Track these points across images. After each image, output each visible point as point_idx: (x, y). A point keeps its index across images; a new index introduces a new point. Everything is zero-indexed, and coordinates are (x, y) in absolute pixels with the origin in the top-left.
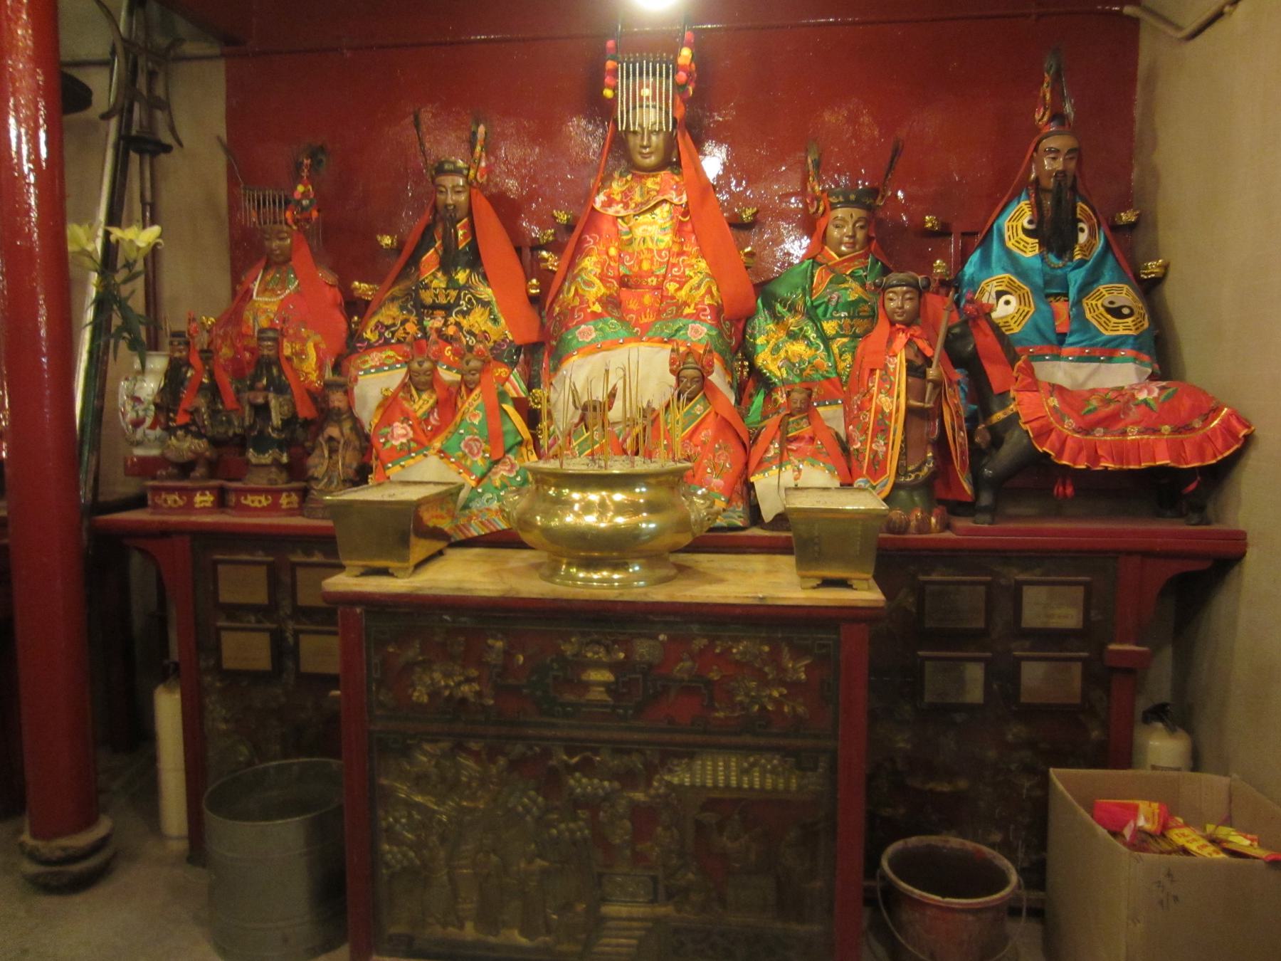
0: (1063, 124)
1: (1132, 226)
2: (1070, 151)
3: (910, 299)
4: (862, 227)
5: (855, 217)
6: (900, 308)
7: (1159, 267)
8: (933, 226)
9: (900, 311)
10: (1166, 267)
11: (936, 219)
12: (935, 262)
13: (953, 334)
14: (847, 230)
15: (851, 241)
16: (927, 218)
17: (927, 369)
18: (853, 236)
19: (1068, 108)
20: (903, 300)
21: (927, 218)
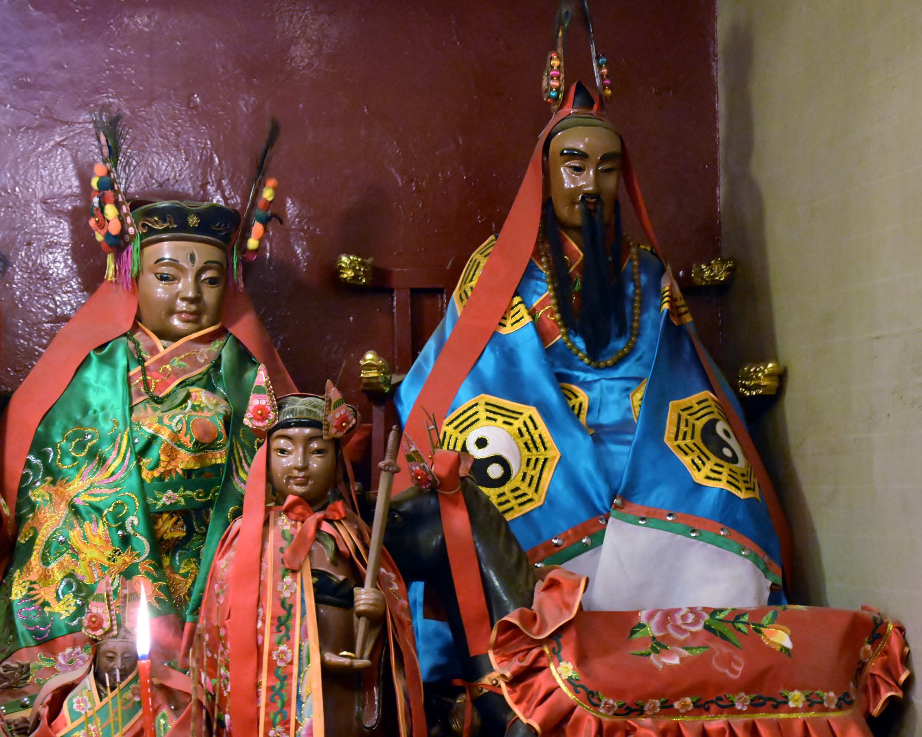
0: (588, 102)
1: (720, 289)
2: (605, 158)
3: (319, 451)
4: (212, 281)
5: (199, 263)
6: (300, 470)
7: (769, 375)
8: (356, 277)
9: (302, 474)
10: (781, 377)
11: (362, 264)
12: (362, 356)
13: (400, 513)
14: (185, 286)
15: (193, 308)
16: (344, 259)
17: (356, 590)
18: (197, 300)
19: (599, 71)
20: (307, 453)
21: (344, 259)
